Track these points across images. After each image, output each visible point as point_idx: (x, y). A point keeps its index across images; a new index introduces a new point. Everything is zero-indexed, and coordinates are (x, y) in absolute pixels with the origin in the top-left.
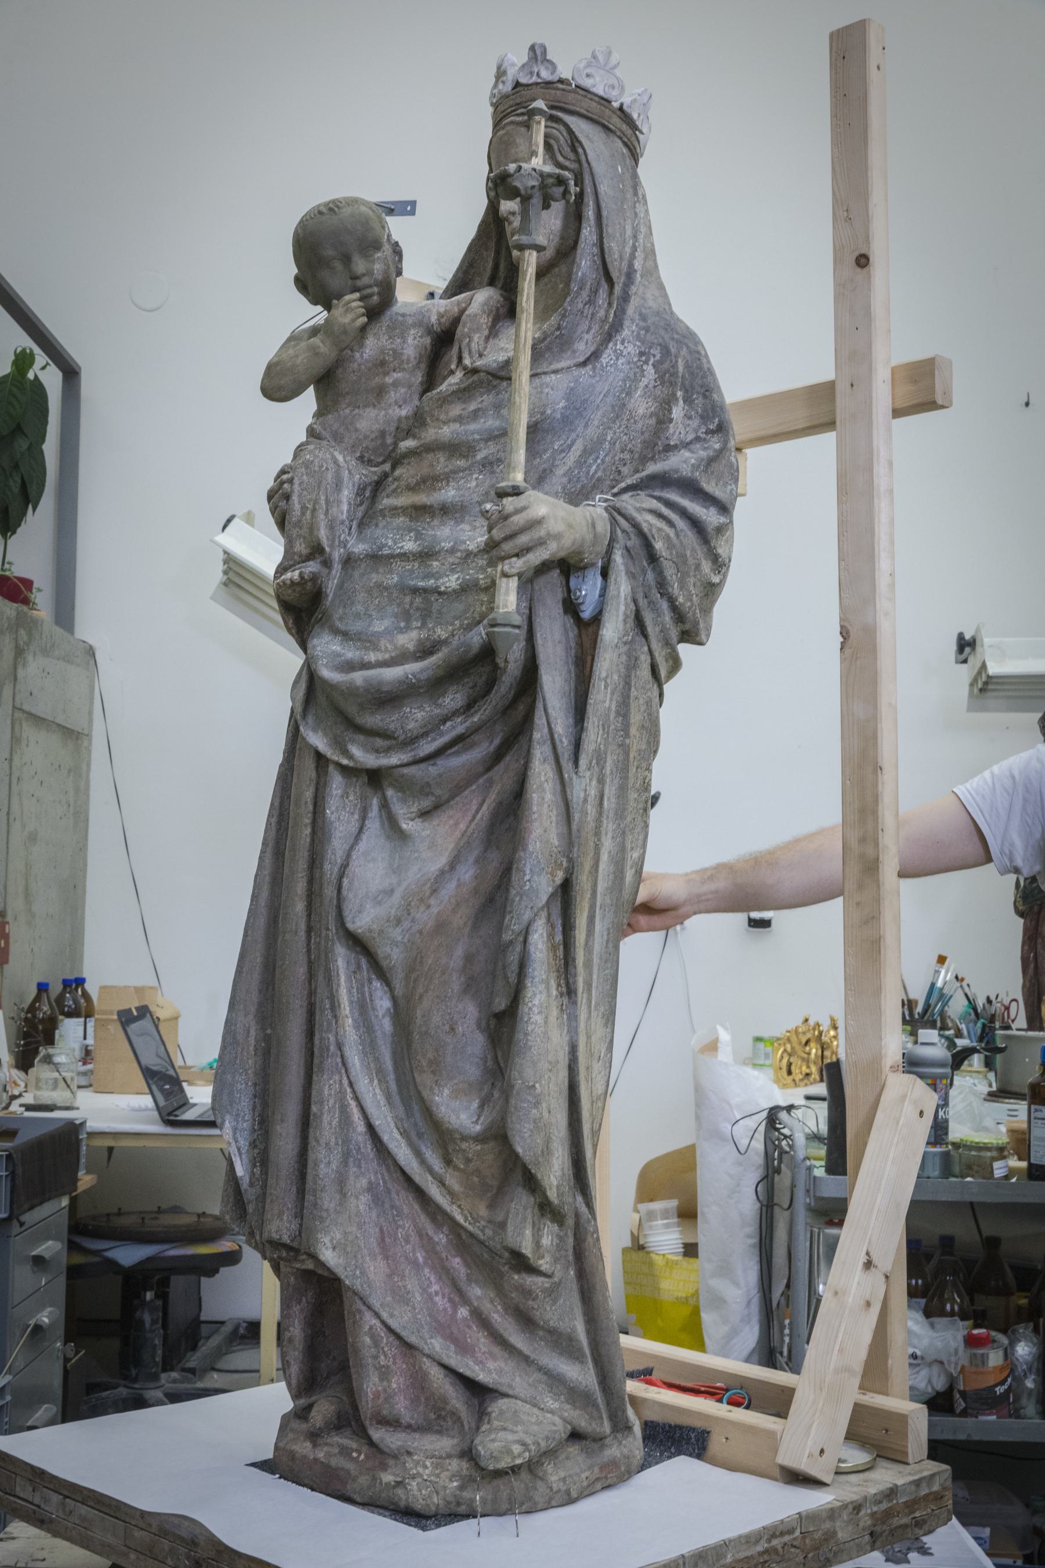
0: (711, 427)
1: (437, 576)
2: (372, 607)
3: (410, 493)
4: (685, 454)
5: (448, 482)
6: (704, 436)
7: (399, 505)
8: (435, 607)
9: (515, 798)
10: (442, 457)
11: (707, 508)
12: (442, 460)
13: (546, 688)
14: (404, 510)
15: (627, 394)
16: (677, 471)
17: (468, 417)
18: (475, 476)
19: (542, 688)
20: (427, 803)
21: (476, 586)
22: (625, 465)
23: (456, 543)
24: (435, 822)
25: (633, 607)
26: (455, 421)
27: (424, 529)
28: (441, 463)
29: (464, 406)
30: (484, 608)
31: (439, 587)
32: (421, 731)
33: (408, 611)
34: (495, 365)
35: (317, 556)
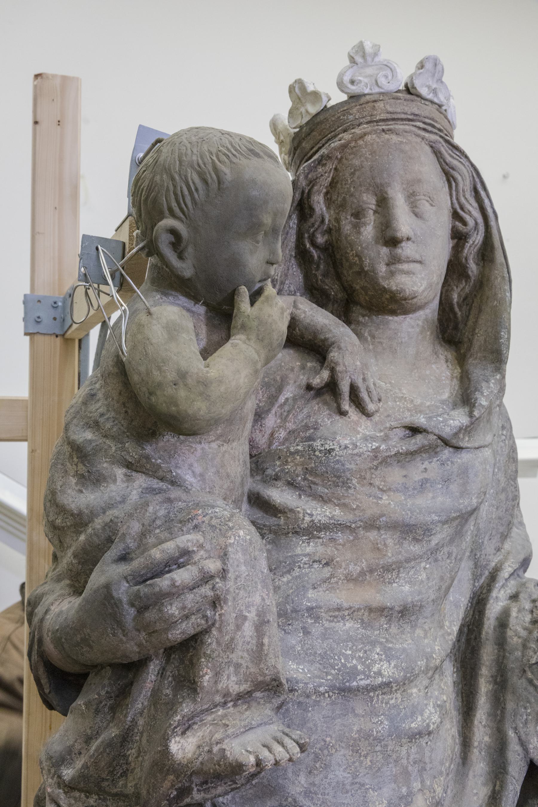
2: (363, 771)
3: (351, 585)
7: (345, 605)
8: (427, 754)
10: (389, 539)
14: (352, 612)
15: (499, 470)
17: (414, 489)
18: (423, 564)
23: (427, 659)
26: (397, 490)
27: (387, 641)
28: (393, 547)
29: (404, 473)
31: (428, 725)
33: (407, 767)
34: (448, 430)
35: (258, 694)
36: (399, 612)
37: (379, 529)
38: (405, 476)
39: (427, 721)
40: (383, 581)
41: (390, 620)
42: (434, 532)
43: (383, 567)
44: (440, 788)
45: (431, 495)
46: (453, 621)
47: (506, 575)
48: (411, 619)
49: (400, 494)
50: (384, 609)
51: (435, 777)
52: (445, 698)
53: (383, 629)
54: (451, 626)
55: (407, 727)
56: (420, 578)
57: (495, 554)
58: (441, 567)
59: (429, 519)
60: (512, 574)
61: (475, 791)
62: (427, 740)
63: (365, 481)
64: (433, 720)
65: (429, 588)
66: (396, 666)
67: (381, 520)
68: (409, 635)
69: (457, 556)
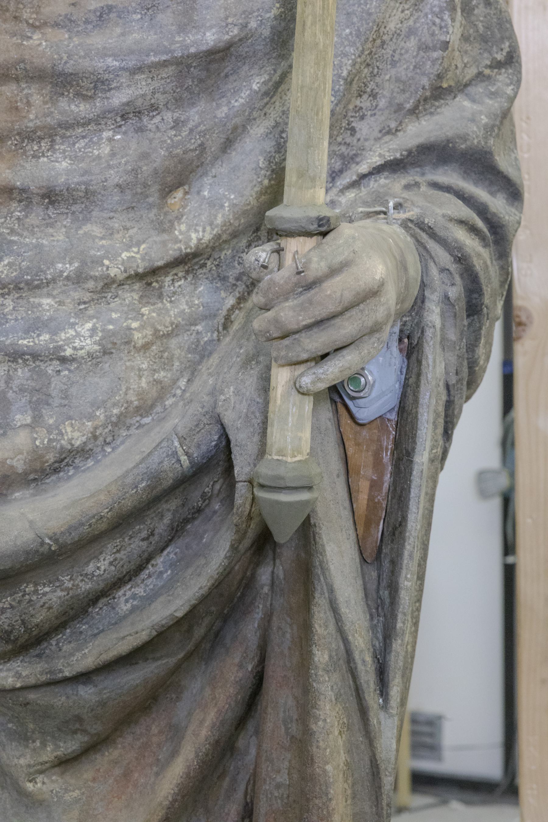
0: (500, 57)
1: (53, 326)
4: (463, 103)
5: (53, 141)
6: (487, 72)
8: (56, 385)
9: (236, 729)
10: (36, 95)
11: (492, 194)
12: (37, 99)
13: (332, 567)
16: (464, 138)
18: (106, 134)
19: (324, 570)
20: (70, 746)
21: (128, 343)
22: (362, 118)
23: (83, 263)
24: (88, 775)
25: (444, 398)
26: (56, 25)
27: (13, 231)
28: (38, 106)
30: (144, 383)
31: (60, 348)
32: (58, 622)
36: (43, 196)
37: (17, 80)
38: (73, 4)
39: (61, 343)
40: (25, 153)
41: (27, 206)
42: (114, 85)
43: (19, 134)
44: (76, 434)
45: (118, 30)
46: (197, 225)
47: (364, 168)
48: (73, 208)
49: (62, 31)
50: (12, 190)
51: (70, 418)
52: (135, 325)
53: (11, 217)
54: (188, 230)
55: (8, 342)
56: (96, 152)
57: (377, 139)
58: (151, 141)
59: (100, 65)
60: (378, 170)
61: (144, 449)
62: (59, 368)
63: (8, 14)
64: (76, 344)
65: (109, 167)
66: (10, 264)
67: (18, 67)
68: (64, 230)
69: (196, 127)
